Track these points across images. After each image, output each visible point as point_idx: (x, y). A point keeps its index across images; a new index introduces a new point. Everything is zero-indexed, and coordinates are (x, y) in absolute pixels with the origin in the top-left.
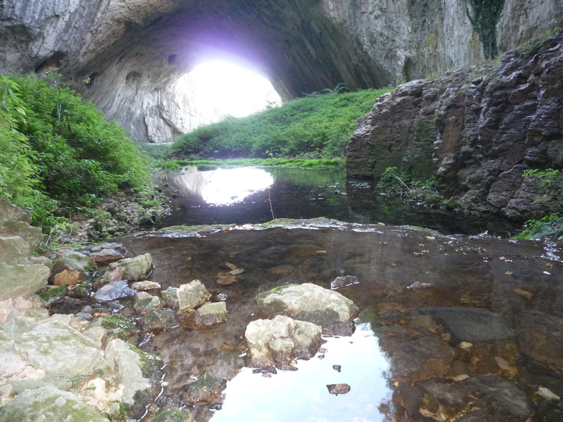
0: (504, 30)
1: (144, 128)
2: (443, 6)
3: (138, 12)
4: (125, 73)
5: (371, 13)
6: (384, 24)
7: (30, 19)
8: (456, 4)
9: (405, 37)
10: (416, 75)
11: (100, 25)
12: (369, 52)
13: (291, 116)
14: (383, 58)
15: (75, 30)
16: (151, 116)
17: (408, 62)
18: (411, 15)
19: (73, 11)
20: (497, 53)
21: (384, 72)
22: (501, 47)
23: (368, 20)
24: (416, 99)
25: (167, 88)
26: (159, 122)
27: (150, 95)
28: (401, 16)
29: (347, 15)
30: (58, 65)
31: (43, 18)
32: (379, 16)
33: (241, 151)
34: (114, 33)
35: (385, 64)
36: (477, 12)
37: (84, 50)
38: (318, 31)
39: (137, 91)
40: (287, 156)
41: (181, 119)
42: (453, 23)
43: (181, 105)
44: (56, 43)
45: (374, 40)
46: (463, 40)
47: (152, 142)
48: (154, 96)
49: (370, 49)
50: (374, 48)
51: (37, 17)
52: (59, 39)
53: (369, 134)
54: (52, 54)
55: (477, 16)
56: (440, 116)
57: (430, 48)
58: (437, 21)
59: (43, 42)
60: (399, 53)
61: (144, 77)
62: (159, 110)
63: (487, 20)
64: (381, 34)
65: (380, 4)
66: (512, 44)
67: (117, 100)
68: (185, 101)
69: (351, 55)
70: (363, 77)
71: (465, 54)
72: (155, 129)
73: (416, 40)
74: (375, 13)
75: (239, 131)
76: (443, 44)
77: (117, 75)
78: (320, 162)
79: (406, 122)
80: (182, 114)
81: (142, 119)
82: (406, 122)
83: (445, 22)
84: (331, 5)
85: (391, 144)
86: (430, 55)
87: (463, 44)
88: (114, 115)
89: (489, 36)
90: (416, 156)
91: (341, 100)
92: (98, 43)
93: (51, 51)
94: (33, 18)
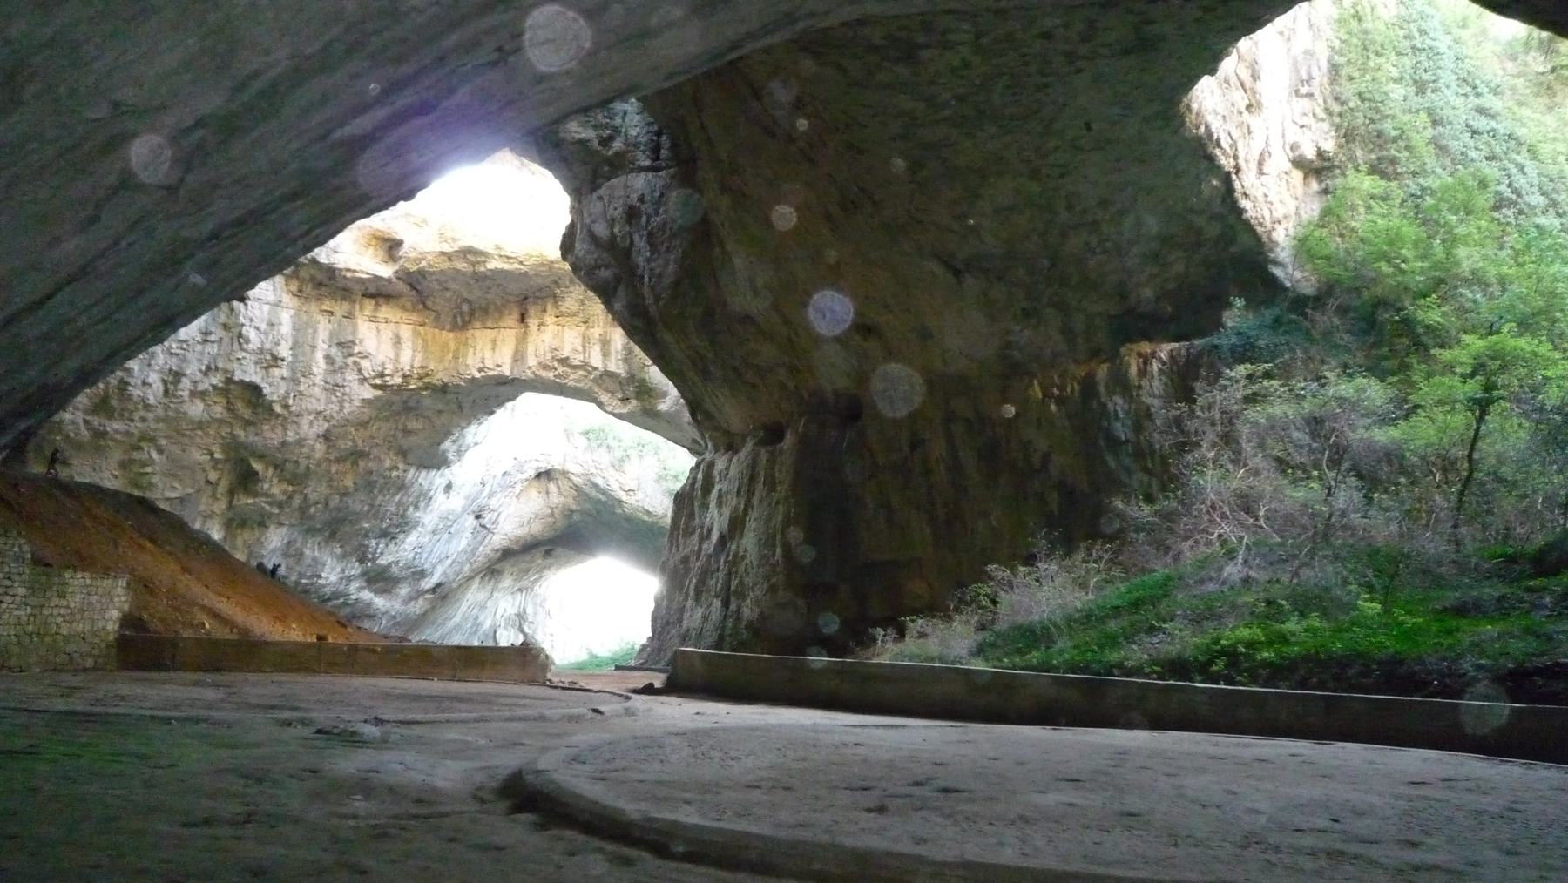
27: (509, 598)
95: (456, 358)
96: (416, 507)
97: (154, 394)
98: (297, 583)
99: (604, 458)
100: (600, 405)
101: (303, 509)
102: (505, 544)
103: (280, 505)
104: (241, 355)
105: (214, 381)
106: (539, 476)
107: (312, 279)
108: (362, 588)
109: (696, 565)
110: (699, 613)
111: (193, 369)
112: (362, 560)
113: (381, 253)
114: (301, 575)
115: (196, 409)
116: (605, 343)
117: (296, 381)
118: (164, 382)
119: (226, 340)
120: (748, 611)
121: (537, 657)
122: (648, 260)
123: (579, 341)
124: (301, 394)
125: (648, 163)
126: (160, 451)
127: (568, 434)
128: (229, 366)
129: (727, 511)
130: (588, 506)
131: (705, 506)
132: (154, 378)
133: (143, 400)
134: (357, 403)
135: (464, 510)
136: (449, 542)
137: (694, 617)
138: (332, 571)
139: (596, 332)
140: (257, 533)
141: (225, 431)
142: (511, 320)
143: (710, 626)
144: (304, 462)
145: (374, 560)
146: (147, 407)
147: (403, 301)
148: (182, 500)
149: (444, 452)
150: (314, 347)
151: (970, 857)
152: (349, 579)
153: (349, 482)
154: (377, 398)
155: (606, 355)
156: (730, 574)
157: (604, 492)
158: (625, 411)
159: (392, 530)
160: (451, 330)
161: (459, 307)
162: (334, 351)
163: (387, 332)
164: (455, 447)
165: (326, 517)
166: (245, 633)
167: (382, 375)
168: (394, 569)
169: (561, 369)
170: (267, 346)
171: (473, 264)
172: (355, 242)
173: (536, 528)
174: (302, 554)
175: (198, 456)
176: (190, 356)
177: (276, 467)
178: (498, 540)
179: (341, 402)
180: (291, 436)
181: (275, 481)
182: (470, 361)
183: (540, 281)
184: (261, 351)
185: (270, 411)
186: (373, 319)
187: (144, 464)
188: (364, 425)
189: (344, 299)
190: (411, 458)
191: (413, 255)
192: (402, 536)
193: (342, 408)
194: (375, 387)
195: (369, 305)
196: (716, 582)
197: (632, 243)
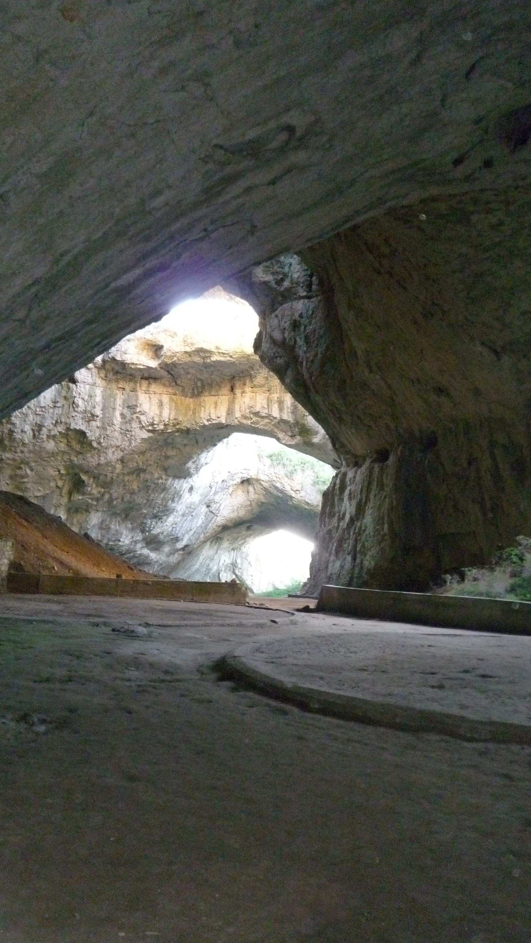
16: (225, 571)
19: (198, 525)
25: (242, 548)
27: (227, 553)
34: (215, 532)
37: (198, 542)
41: (252, 576)
48: (230, 554)
52: (190, 539)
67: (201, 558)
81: (217, 575)
88: (196, 570)
92: (206, 537)
95: (194, 413)
96: (173, 501)
97: (28, 438)
98: (107, 544)
99: (281, 471)
100: (278, 439)
101: (110, 501)
102: (223, 522)
103: (97, 500)
104: (74, 414)
105: (60, 429)
106: (243, 482)
107: (113, 369)
108: (143, 547)
109: (336, 535)
110: (338, 564)
111: (48, 422)
112: (143, 531)
113: (151, 354)
114: (109, 540)
115: (50, 445)
116: (281, 403)
117: (104, 428)
118: (33, 430)
119: (66, 406)
120: (369, 562)
121: (240, 589)
122: (305, 352)
123: (265, 401)
124: (107, 435)
125: (305, 294)
126: (32, 470)
127: (260, 457)
128: (68, 421)
129: (354, 503)
130: (272, 500)
131: (341, 500)
132: (27, 428)
133: (22, 441)
134: (139, 441)
135: (200, 502)
136: (192, 521)
137: (335, 566)
138: (126, 538)
139: (275, 396)
140: (84, 516)
141: (66, 458)
142: (226, 390)
143: (344, 572)
144: (109, 475)
145: (149, 531)
146: (24, 444)
147: (164, 381)
148: (44, 497)
149: (188, 469)
150: (114, 409)
151: (495, 718)
152: (136, 542)
153: (135, 487)
154: (150, 438)
155: (281, 409)
156: (356, 540)
157: (282, 491)
158: (293, 443)
159: (159, 514)
160: (192, 397)
161: (196, 384)
162: (125, 411)
163: (155, 399)
164: (194, 466)
165: (122, 506)
166: (77, 573)
167: (152, 424)
168: (161, 537)
169: (255, 419)
170: (88, 409)
171: (204, 359)
172: (136, 348)
173: (242, 513)
174: (109, 528)
175: (52, 472)
176: (46, 415)
177: (94, 478)
178: (220, 520)
179: (130, 441)
180: (103, 460)
181: (94, 486)
182: (202, 415)
183: (242, 367)
184: (85, 411)
185: (90, 445)
186: (147, 392)
187: (22, 477)
188: (143, 453)
189: (131, 380)
190: (169, 472)
191: (169, 354)
192: (165, 518)
193: (131, 443)
194: (149, 431)
195: (145, 383)
196: (348, 545)
197: (295, 342)
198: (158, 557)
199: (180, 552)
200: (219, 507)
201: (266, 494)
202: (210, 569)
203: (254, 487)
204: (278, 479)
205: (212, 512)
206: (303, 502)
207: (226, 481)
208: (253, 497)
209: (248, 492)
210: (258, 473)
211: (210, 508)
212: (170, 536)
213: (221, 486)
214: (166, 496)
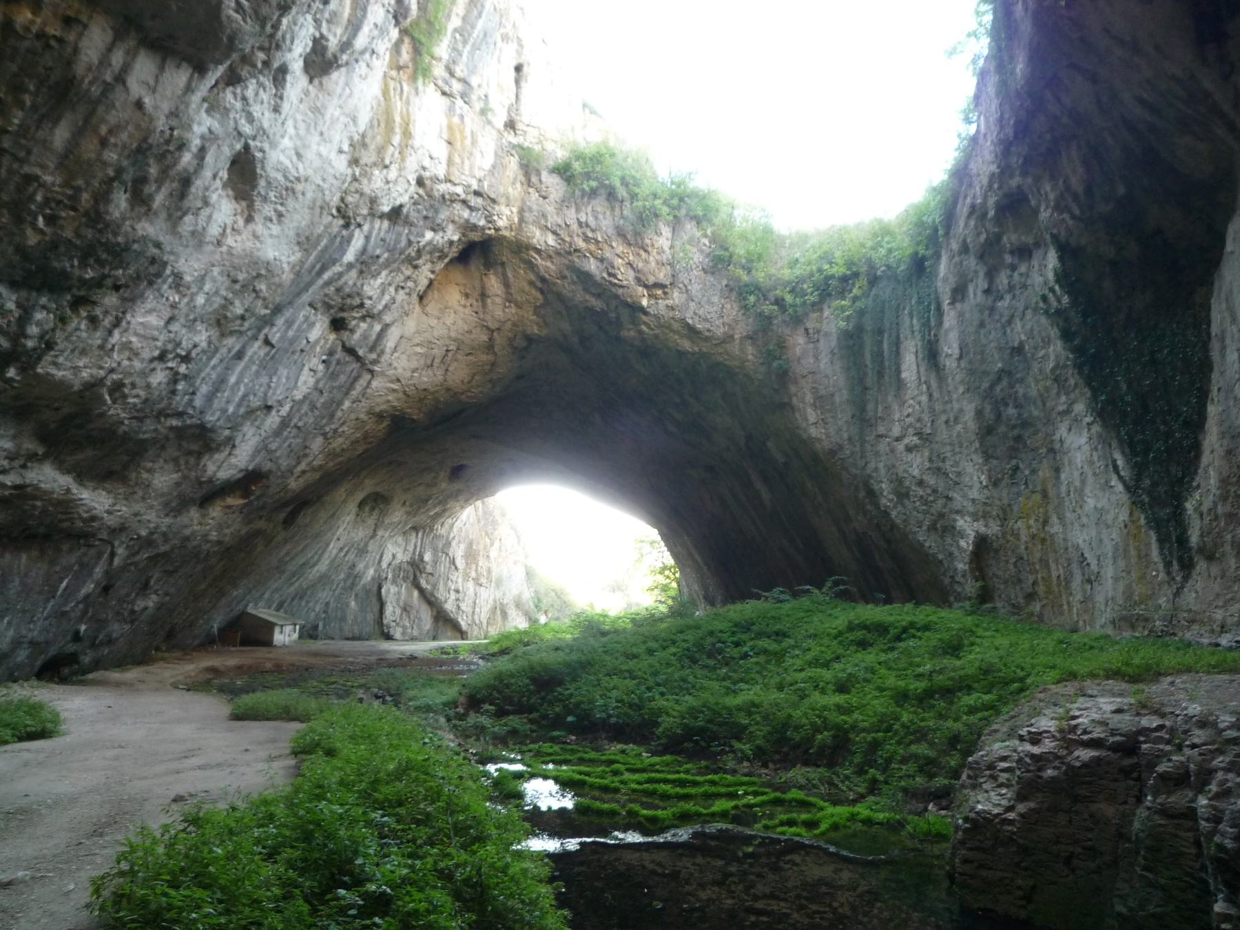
0: (1207, 519)
1: (376, 609)
2: (1057, 446)
3: (421, 400)
4: (360, 496)
5: (898, 439)
6: (927, 465)
7: (218, 413)
8: (1087, 448)
9: (974, 494)
10: (1000, 573)
11: (343, 424)
12: (894, 514)
13: (737, 644)
14: (925, 528)
15: (295, 431)
16: (394, 582)
17: (982, 544)
18: (983, 452)
19: (298, 395)
20: (1191, 559)
21: (927, 555)
22: (1201, 550)
23: (892, 451)
24: (1127, 762)
26: (410, 595)
27: (400, 539)
28: (965, 452)
29: (845, 436)
30: (245, 496)
31: (242, 410)
32: (916, 446)
33: (628, 725)
35: (930, 543)
36: (1139, 470)
37: (303, 466)
38: (780, 458)
39: (375, 530)
40: (745, 764)
42: (1083, 482)
43: (460, 563)
44: (253, 456)
45: (903, 491)
46: (1109, 518)
47: (388, 637)
48: (407, 541)
49: (895, 507)
50: (904, 507)
51: (231, 409)
52: (263, 448)
53: (1011, 816)
54: (240, 475)
55: (1138, 478)
56: (1220, 847)
57: (1031, 522)
58: (1044, 472)
59: (230, 454)
60: (961, 523)
61: (396, 504)
62: (414, 571)
63: (1161, 489)
64: (921, 483)
65: (918, 425)
66: (1228, 548)
67: (333, 548)
68: (471, 556)
69: (852, 512)
70: (877, 557)
71: (1116, 548)
72: (398, 611)
73: (998, 503)
74: (906, 441)
75: (622, 672)
76: (1061, 518)
77: (345, 502)
78: (853, 817)
79: (1108, 810)
80: (460, 580)
81: (375, 588)
82: (1108, 810)
83: (1063, 476)
84: (812, 416)
85: (1072, 853)
86: (1033, 537)
87: (1108, 527)
88: (321, 577)
89: (1168, 521)
90: (1151, 908)
91: (851, 628)
92: (332, 455)
93: (241, 471)
94: (224, 411)
96: (140, 199)
99: (602, 219)
127: (529, 168)
130: (566, 326)
135: (304, 278)
136: (268, 366)
157: (605, 290)
159: (69, 265)
173: (459, 374)
178: (380, 390)
192: (111, 300)
198: (124, 510)
199: (230, 501)
200: (381, 335)
201: (546, 303)
202: (358, 577)
203: (505, 275)
204: (592, 247)
205: (351, 351)
206: (676, 326)
207: (408, 223)
208: (499, 313)
209: (483, 296)
210: (521, 220)
211: (345, 335)
212: (162, 414)
213: (391, 238)
214: (89, 148)
